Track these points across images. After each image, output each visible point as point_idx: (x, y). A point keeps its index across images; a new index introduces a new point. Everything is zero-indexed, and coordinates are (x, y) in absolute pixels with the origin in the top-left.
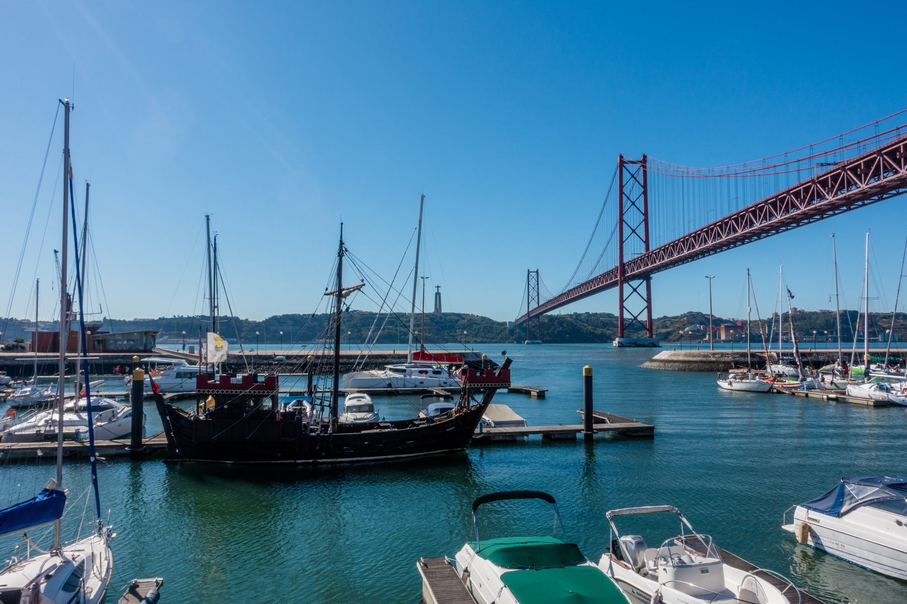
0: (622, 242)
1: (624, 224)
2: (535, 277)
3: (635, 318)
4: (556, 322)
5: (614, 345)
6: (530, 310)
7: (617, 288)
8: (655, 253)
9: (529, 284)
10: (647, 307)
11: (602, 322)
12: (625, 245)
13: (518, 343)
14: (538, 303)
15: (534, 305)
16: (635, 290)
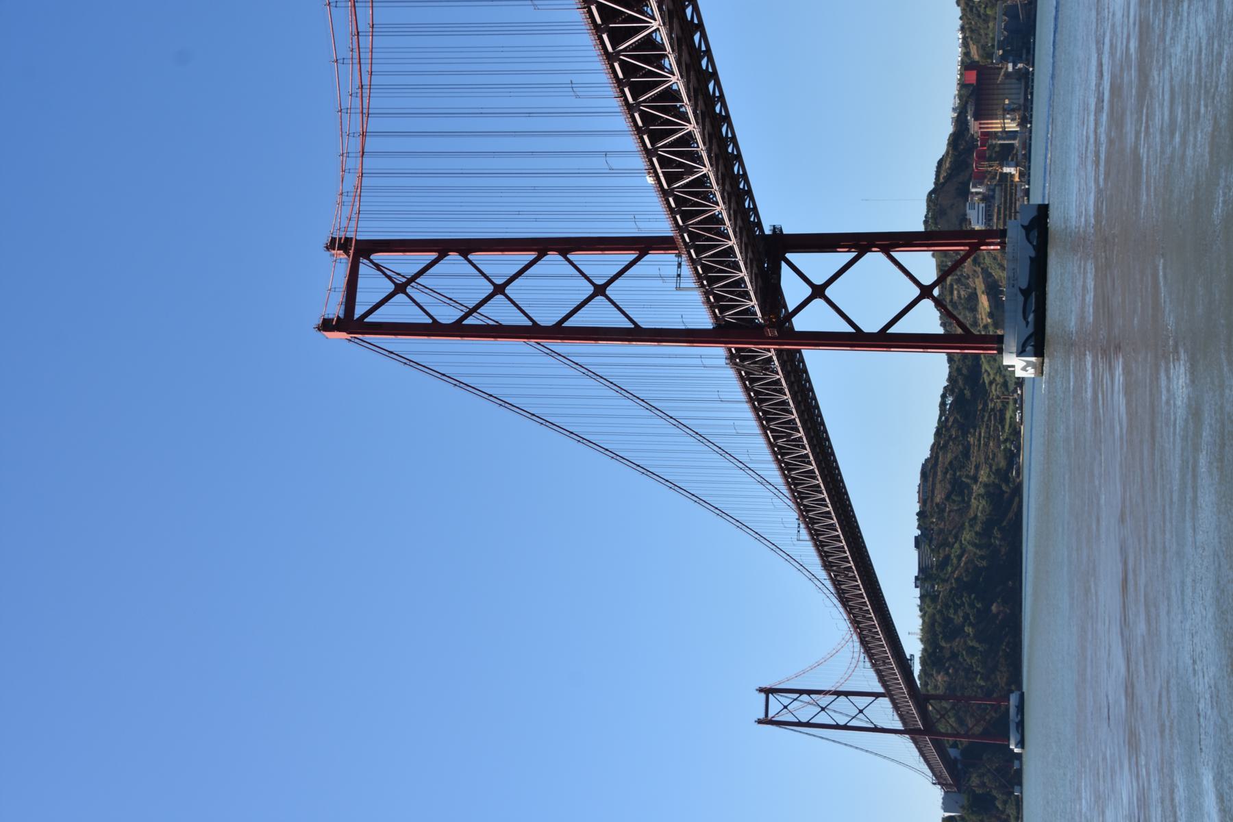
0: (636, 334)
1: (573, 322)
2: (786, 702)
3: (926, 292)
4: (943, 644)
5: (1030, 373)
6: (899, 725)
7: (813, 358)
8: (671, 178)
9: (808, 724)
10: (886, 250)
11: (948, 497)
12: (647, 321)
13: (1020, 784)
14: (877, 695)
16: (818, 292)
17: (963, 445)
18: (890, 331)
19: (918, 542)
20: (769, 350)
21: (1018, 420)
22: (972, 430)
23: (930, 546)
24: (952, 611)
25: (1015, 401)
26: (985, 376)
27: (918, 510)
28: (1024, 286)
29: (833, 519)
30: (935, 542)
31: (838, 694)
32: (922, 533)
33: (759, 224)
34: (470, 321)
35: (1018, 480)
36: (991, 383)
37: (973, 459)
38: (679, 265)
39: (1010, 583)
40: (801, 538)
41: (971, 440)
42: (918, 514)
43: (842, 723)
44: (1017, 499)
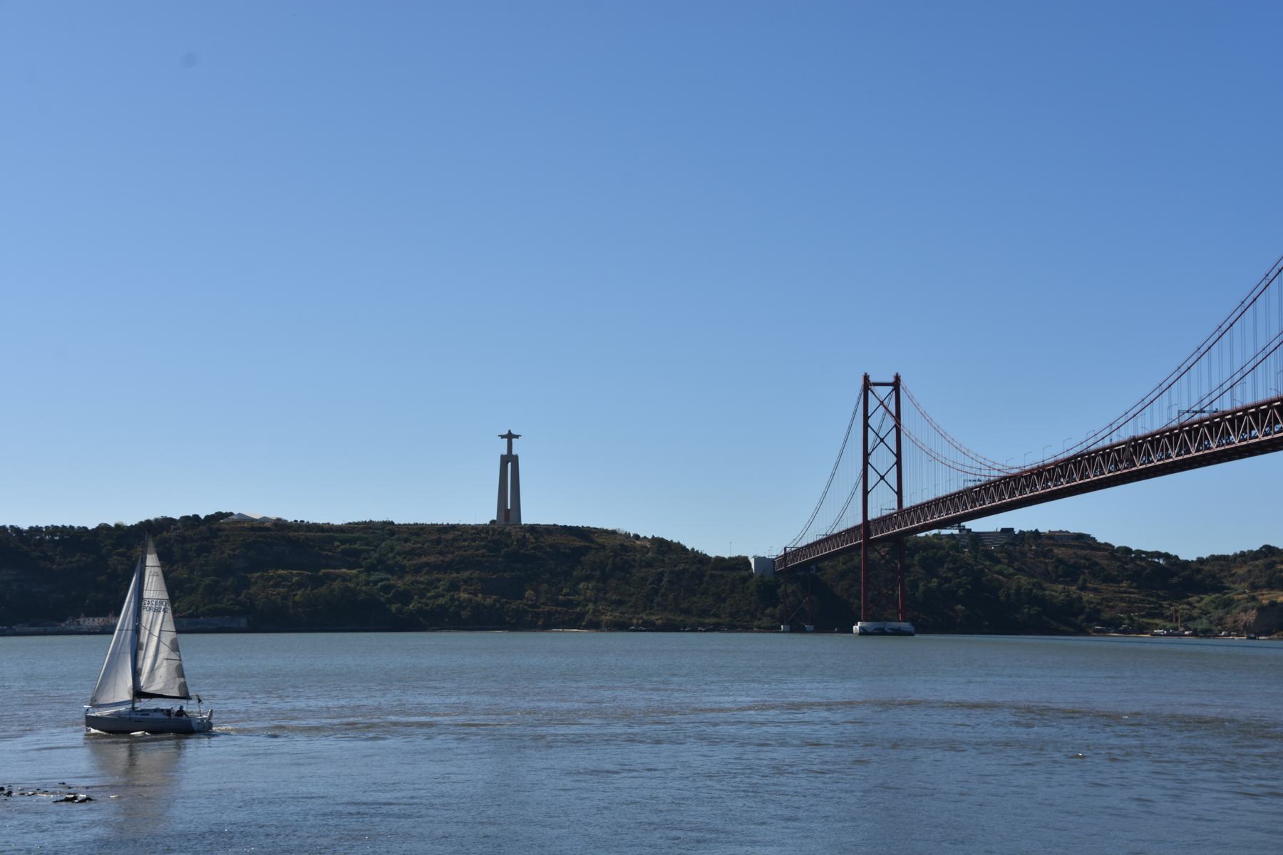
4: (917, 558)
6: (873, 514)
9: (866, 426)
11: (1060, 561)
13: (792, 631)
15: (881, 504)
17: (1118, 576)
21: (1155, 631)
22: (1135, 584)
23: (1006, 543)
24: (951, 566)
25: (1176, 629)
26: (1196, 598)
27: (1040, 531)
29: (1198, 450)
30: (1011, 548)
32: (1017, 535)
35: (1091, 631)
36: (1189, 604)
37: (1104, 586)
39: (987, 623)
41: (1124, 584)
42: (1037, 530)
44: (1072, 630)
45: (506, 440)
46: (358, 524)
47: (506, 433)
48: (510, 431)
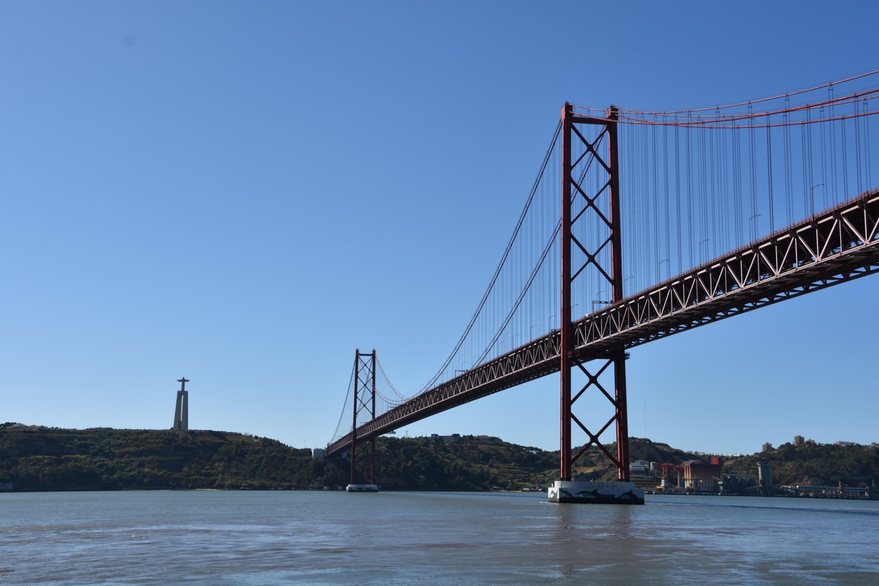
3: (594, 438)
4: (402, 449)
5: (550, 495)
6: (358, 426)
8: (655, 297)
9: (357, 377)
10: (617, 417)
11: (481, 452)
12: (575, 285)
13: (330, 489)
14: (373, 414)
16: (593, 380)
17: (510, 460)
18: (572, 419)
19: (456, 436)
20: (560, 353)
22: (518, 464)
23: (454, 442)
24: (420, 454)
25: (535, 488)
26: (548, 471)
27: (474, 436)
28: (599, 492)
29: (467, 389)
30: (456, 445)
31: (374, 393)
33: (630, 346)
34: (573, 187)
35: (491, 489)
36: (544, 474)
37: (502, 465)
38: (606, 303)
39: (436, 485)
40: (457, 372)
41: (513, 464)
42: (471, 435)
43: (358, 395)
44: (481, 489)
45: (181, 383)
46: (91, 429)
47: (181, 379)
48: (183, 378)
